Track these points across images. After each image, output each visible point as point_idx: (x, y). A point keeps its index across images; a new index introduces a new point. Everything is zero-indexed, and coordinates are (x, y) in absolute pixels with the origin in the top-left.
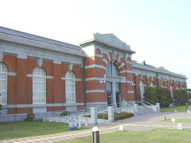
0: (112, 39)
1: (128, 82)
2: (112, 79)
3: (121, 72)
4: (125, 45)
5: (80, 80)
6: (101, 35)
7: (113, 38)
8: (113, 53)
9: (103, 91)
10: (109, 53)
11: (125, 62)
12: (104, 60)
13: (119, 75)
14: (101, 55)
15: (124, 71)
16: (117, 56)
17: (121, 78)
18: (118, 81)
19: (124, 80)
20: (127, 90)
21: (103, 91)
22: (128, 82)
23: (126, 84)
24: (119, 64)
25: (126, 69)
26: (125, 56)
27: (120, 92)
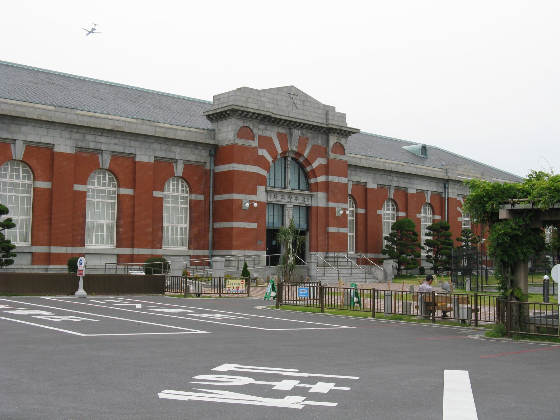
0: (292, 101)
1: (332, 205)
2: (283, 198)
3: (313, 181)
4: (330, 113)
5: (201, 197)
6: (258, 91)
7: (292, 96)
8: (291, 135)
9: (254, 225)
10: (279, 135)
11: (325, 155)
12: (263, 152)
13: (309, 187)
14: (254, 140)
15: (321, 179)
16: (303, 143)
17: (312, 196)
18: (300, 202)
19: (320, 200)
20: (327, 225)
21: (254, 225)
22: (332, 205)
23: (327, 209)
24: (306, 160)
25: (327, 174)
26: (328, 141)
27: (308, 230)
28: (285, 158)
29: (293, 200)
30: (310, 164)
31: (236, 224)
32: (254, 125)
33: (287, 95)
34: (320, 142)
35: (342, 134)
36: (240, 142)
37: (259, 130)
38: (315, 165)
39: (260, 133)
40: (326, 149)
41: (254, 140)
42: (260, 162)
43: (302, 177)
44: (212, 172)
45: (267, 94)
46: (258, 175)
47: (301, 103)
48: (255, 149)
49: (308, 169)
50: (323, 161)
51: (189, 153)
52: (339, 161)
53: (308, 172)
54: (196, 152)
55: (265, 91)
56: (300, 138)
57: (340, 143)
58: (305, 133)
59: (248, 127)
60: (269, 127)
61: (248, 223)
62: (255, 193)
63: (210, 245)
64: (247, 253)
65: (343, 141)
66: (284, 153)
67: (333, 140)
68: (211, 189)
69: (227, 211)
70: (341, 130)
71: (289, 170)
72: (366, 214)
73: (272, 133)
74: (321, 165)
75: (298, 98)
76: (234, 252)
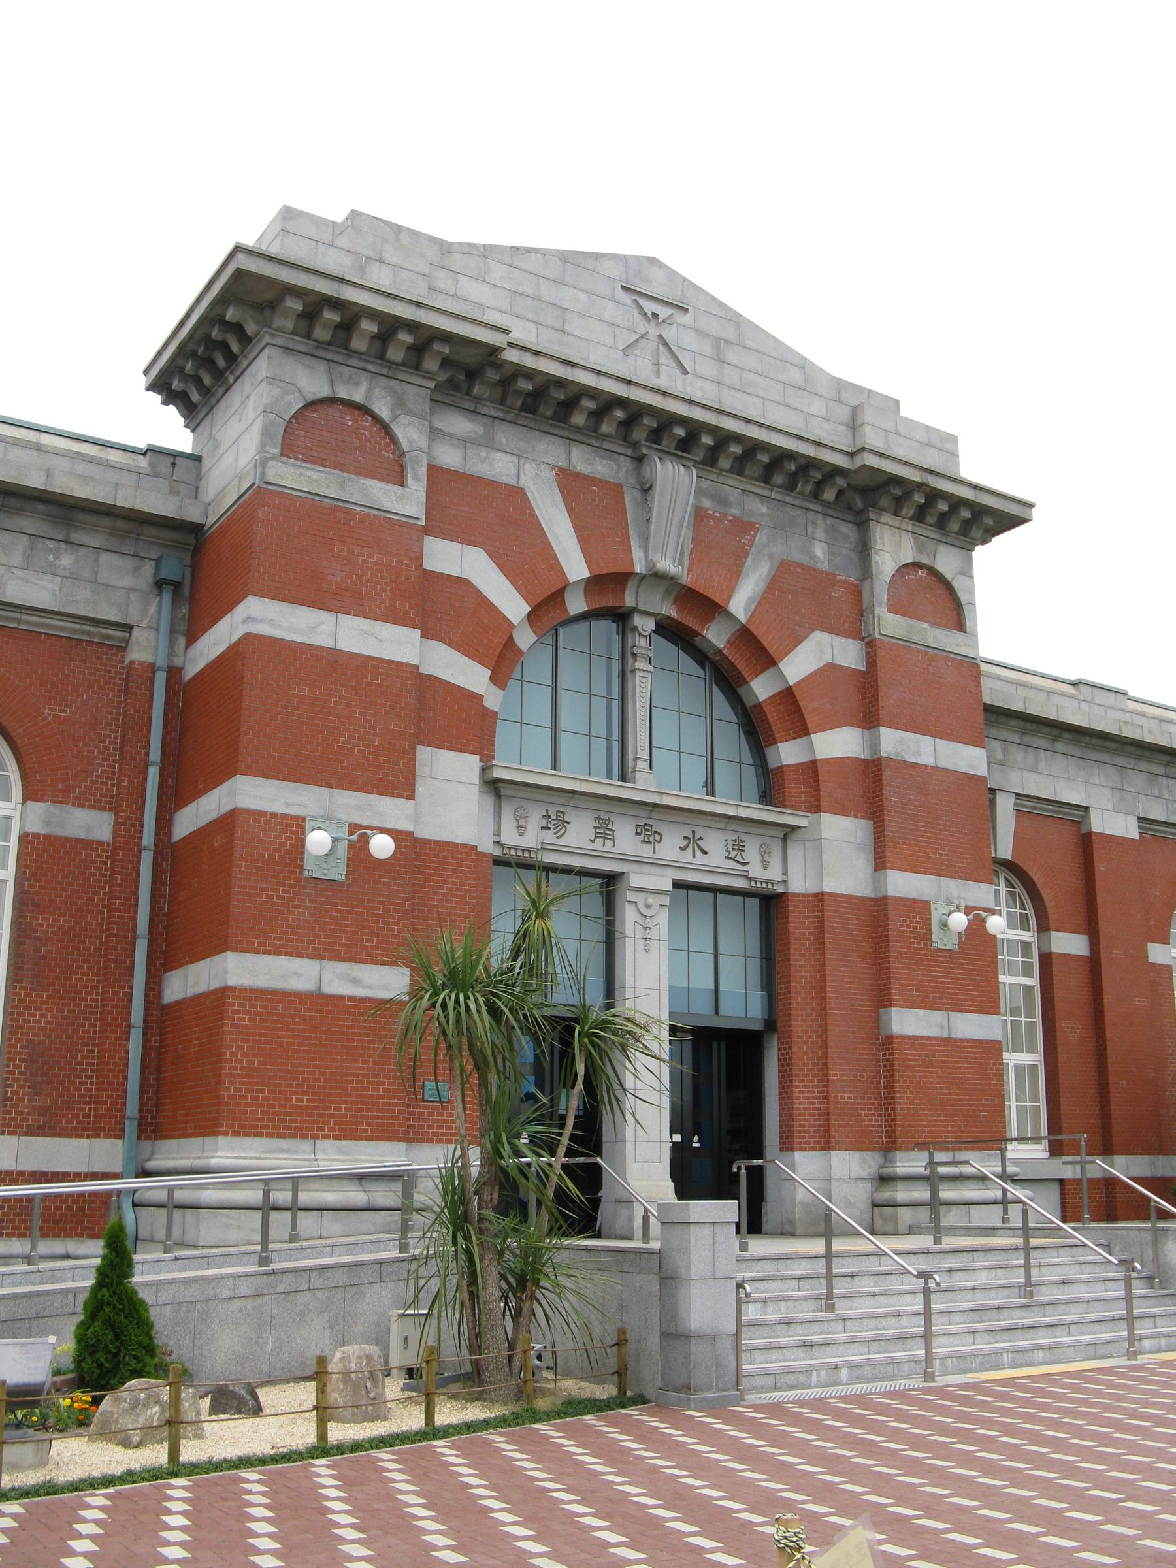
0: (653, 330)
1: (902, 884)
2: (604, 832)
3: (788, 753)
4: (868, 416)
5: (92, 824)
6: (446, 248)
7: (650, 307)
8: (646, 489)
9: (387, 982)
10: (571, 484)
11: (854, 621)
13: (771, 786)
14: (402, 483)
15: (838, 743)
16: (720, 540)
17: (788, 833)
18: (714, 861)
19: (833, 859)
20: (883, 999)
21: (387, 982)
22: (902, 884)
23: (877, 910)
24: (745, 636)
25: (869, 717)
26: (864, 549)
27: (771, 1024)
28: (622, 618)
29: (670, 847)
30: (767, 661)
31: (239, 970)
32: (400, 404)
33: (627, 298)
34: (819, 546)
35: (942, 522)
36: (297, 477)
37: (442, 439)
38: (798, 665)
39: (449, 457)
40: (857, 592)
41: (402, 483)
42: (442, 609)
43: (730, 739)
44: (160, 679)
45: (497, 272)
46: (427, 687)
47: (708, 349)
48: (407, 535)
49: (761, 688)
50: (847, 654)
51: (17, 559)
52: (934, 655)
53: (759, 706)
54: (66, 561)
55: (487, 252)
56: (700, 515)
57: (933, 572)
58: (734, 495)
59: (364, 410)
60: (506, 435)
61: (341, 967)
62: (401, 784)
63: (132, 1108)
64: (332, 1156)
65: (946, 561)
66: (609, 581)
67: (893, 547)
68: (153, 773)
69: (199, 891)
70: (934, 495)
71: (642, 685)
72: (1093, 963)
73: (529, 467)
74: (830, 669)
75: (686, 319)
76: (226, 1151)
